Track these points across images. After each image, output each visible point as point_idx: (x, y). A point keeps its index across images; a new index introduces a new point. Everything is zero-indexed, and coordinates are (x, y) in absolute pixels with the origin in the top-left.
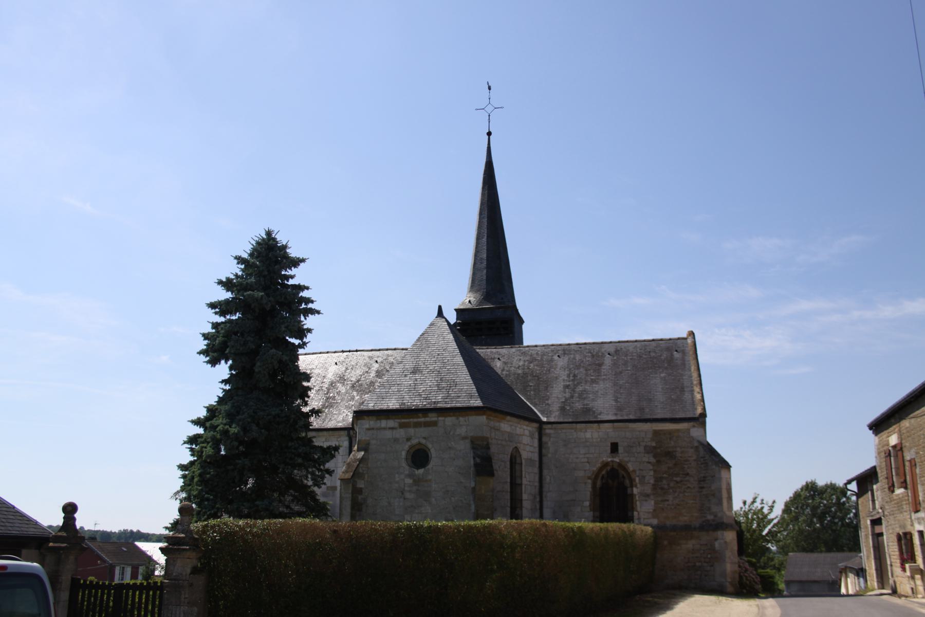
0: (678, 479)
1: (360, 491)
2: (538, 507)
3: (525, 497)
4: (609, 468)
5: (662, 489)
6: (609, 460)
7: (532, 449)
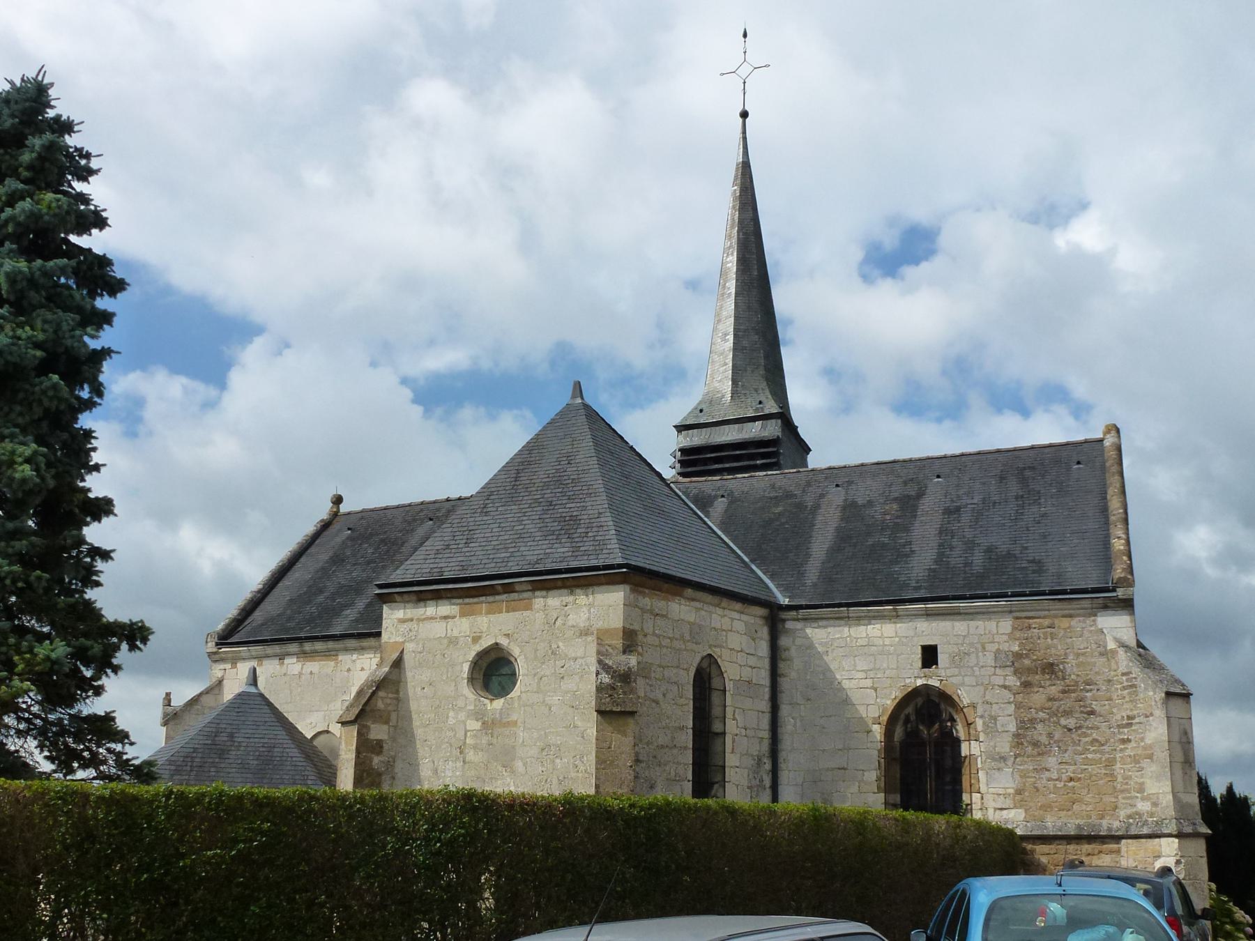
0: (1071, 722)
1: (378, 747)
2: (767, 782)
3: (731, 760)
4: (920, 701)
5: (1036, 744)
6: (919, 682)
7: (752, 661)
